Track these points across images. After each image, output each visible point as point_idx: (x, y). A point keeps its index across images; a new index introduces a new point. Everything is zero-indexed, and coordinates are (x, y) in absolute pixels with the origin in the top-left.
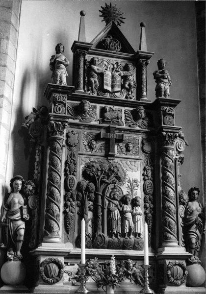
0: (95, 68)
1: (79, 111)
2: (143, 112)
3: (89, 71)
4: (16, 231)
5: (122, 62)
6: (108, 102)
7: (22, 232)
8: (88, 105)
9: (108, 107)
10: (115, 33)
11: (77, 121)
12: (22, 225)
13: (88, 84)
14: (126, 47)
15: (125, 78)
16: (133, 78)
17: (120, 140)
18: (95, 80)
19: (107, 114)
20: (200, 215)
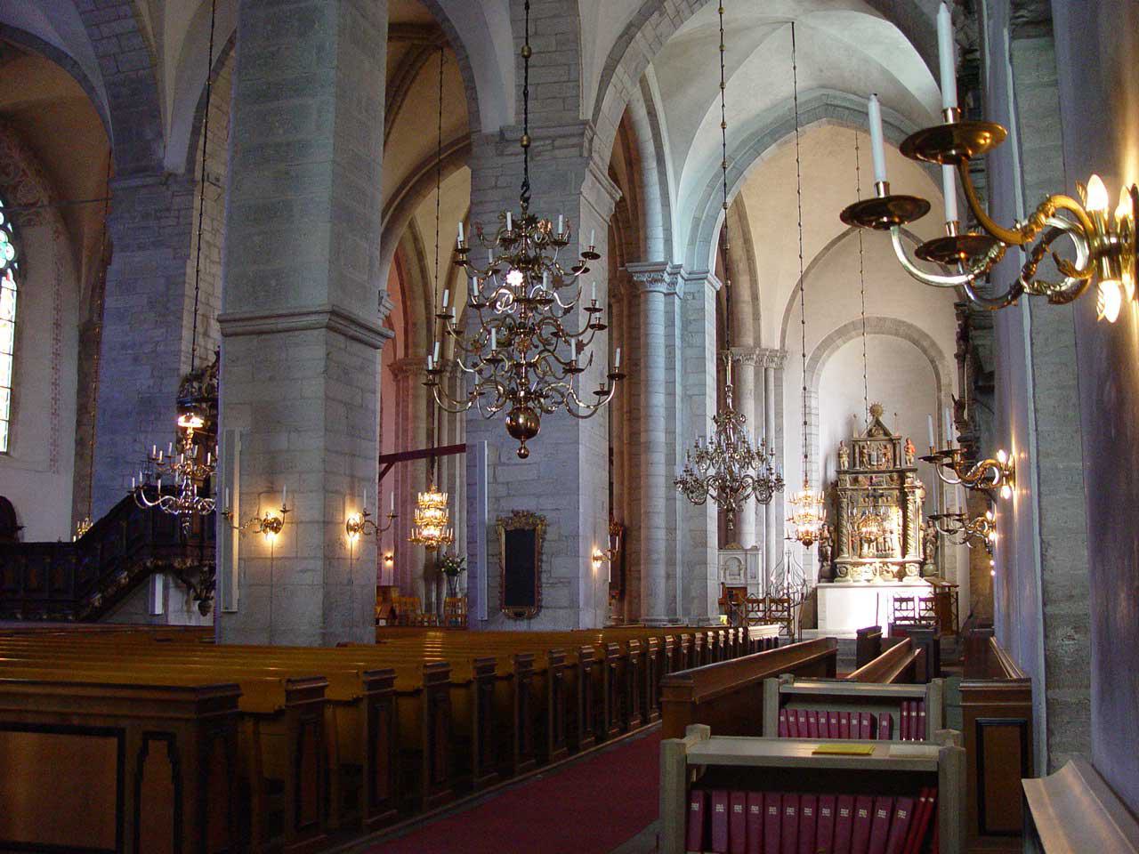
0: (865, 451)
1: (856, 481)
2: (895, 476)
3: (861, 453)
4: (827, 551)
5: (884, 443)
6: (874, 472)
7: (829, 552)
8: (861, 477)
9: (874, 476)
10: (878, 423)
11: (856, 487)
12: (829, 549)
13: (861, 462)
14: (886, 433)
15: (885, 454)
16: (890, 455)
17: (882, 495)
18: (865, 459)
19: (874, 480)
20: (933, 537)
